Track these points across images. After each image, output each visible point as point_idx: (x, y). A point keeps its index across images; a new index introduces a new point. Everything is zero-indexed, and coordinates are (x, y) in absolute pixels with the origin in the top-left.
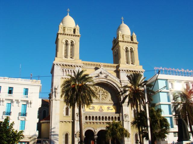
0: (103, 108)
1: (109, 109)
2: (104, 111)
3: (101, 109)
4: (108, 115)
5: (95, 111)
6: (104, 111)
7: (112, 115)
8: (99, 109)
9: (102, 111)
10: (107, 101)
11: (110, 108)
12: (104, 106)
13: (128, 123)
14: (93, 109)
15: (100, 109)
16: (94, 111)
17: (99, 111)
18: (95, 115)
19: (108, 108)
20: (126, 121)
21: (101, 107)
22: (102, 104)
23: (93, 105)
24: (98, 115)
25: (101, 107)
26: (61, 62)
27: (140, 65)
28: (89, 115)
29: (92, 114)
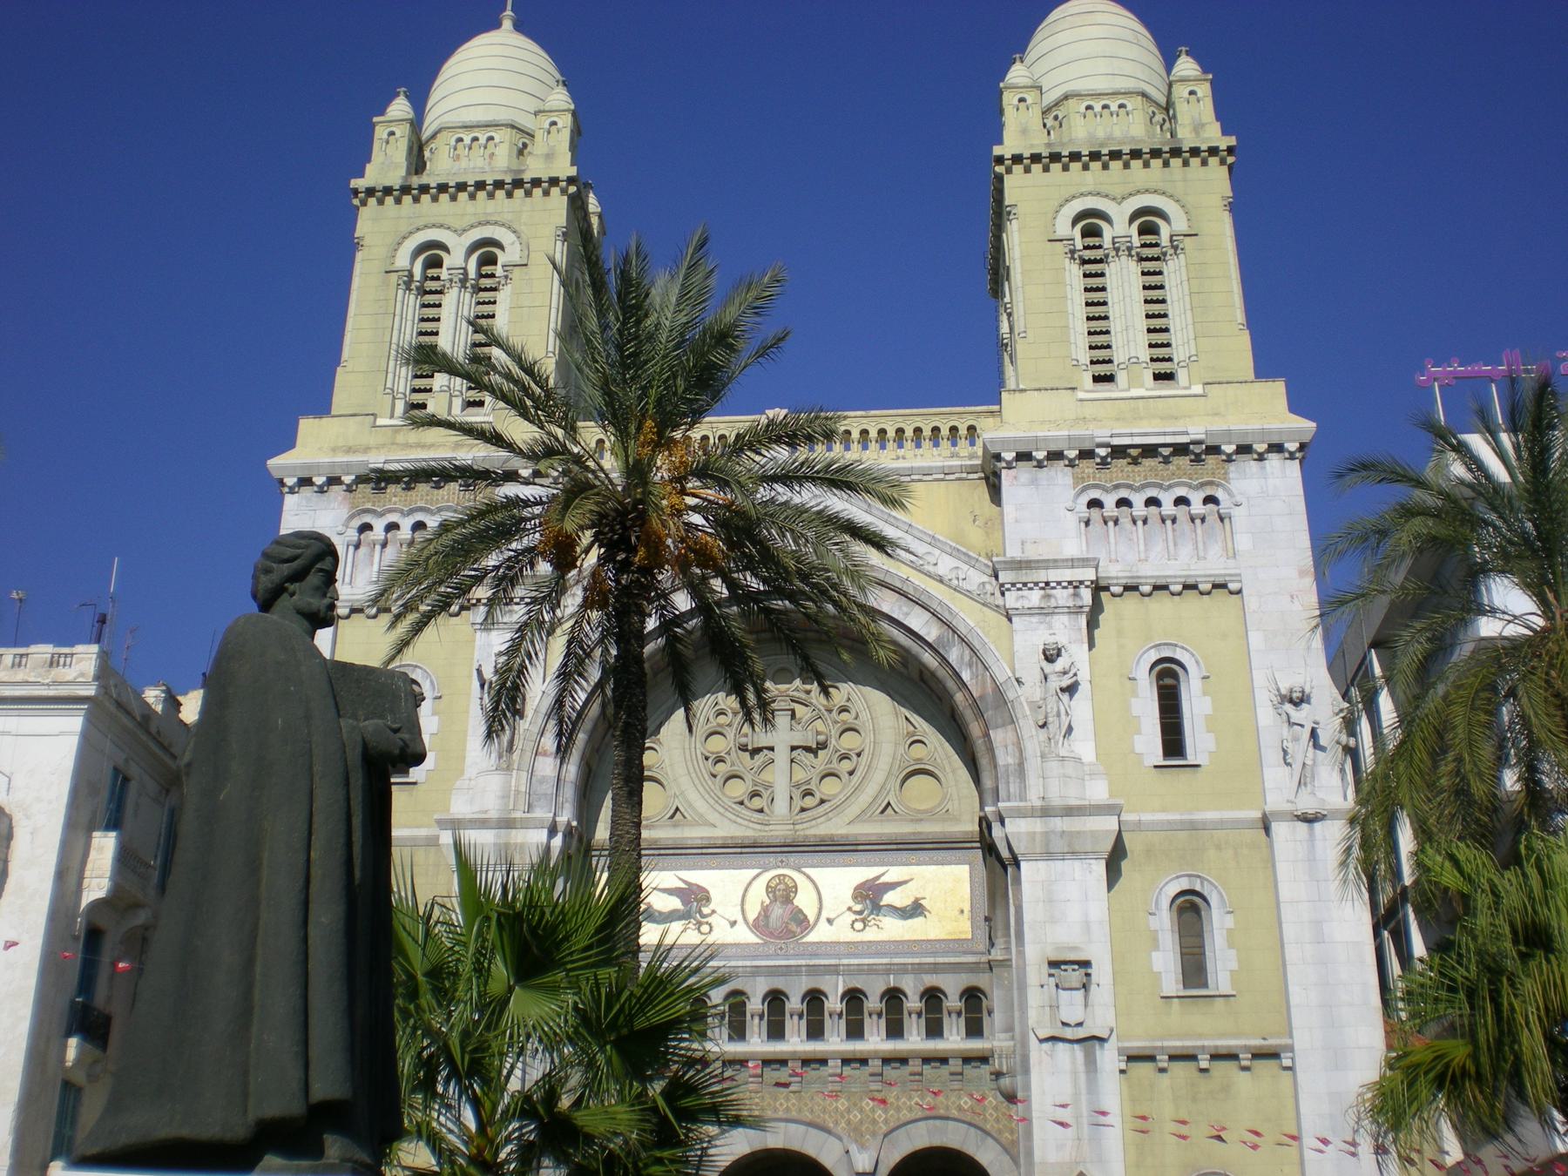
0: (805, 901)
1: (877, 908)
2: (812, 937)
3: (778, 911)
6: (812, 937)
7: (888, 970)
8: (752, 916)
10: (854, 809)
11: (889, 898)
13: (1091, 1063)
15: (765, 911)
16: (692, 937)
19: (870, 897)
20: (1053, 1039)
21: (783, 894)
22: (793, 858)
25: (783, 894)
26: (349, 450)
27: (1264, 369)
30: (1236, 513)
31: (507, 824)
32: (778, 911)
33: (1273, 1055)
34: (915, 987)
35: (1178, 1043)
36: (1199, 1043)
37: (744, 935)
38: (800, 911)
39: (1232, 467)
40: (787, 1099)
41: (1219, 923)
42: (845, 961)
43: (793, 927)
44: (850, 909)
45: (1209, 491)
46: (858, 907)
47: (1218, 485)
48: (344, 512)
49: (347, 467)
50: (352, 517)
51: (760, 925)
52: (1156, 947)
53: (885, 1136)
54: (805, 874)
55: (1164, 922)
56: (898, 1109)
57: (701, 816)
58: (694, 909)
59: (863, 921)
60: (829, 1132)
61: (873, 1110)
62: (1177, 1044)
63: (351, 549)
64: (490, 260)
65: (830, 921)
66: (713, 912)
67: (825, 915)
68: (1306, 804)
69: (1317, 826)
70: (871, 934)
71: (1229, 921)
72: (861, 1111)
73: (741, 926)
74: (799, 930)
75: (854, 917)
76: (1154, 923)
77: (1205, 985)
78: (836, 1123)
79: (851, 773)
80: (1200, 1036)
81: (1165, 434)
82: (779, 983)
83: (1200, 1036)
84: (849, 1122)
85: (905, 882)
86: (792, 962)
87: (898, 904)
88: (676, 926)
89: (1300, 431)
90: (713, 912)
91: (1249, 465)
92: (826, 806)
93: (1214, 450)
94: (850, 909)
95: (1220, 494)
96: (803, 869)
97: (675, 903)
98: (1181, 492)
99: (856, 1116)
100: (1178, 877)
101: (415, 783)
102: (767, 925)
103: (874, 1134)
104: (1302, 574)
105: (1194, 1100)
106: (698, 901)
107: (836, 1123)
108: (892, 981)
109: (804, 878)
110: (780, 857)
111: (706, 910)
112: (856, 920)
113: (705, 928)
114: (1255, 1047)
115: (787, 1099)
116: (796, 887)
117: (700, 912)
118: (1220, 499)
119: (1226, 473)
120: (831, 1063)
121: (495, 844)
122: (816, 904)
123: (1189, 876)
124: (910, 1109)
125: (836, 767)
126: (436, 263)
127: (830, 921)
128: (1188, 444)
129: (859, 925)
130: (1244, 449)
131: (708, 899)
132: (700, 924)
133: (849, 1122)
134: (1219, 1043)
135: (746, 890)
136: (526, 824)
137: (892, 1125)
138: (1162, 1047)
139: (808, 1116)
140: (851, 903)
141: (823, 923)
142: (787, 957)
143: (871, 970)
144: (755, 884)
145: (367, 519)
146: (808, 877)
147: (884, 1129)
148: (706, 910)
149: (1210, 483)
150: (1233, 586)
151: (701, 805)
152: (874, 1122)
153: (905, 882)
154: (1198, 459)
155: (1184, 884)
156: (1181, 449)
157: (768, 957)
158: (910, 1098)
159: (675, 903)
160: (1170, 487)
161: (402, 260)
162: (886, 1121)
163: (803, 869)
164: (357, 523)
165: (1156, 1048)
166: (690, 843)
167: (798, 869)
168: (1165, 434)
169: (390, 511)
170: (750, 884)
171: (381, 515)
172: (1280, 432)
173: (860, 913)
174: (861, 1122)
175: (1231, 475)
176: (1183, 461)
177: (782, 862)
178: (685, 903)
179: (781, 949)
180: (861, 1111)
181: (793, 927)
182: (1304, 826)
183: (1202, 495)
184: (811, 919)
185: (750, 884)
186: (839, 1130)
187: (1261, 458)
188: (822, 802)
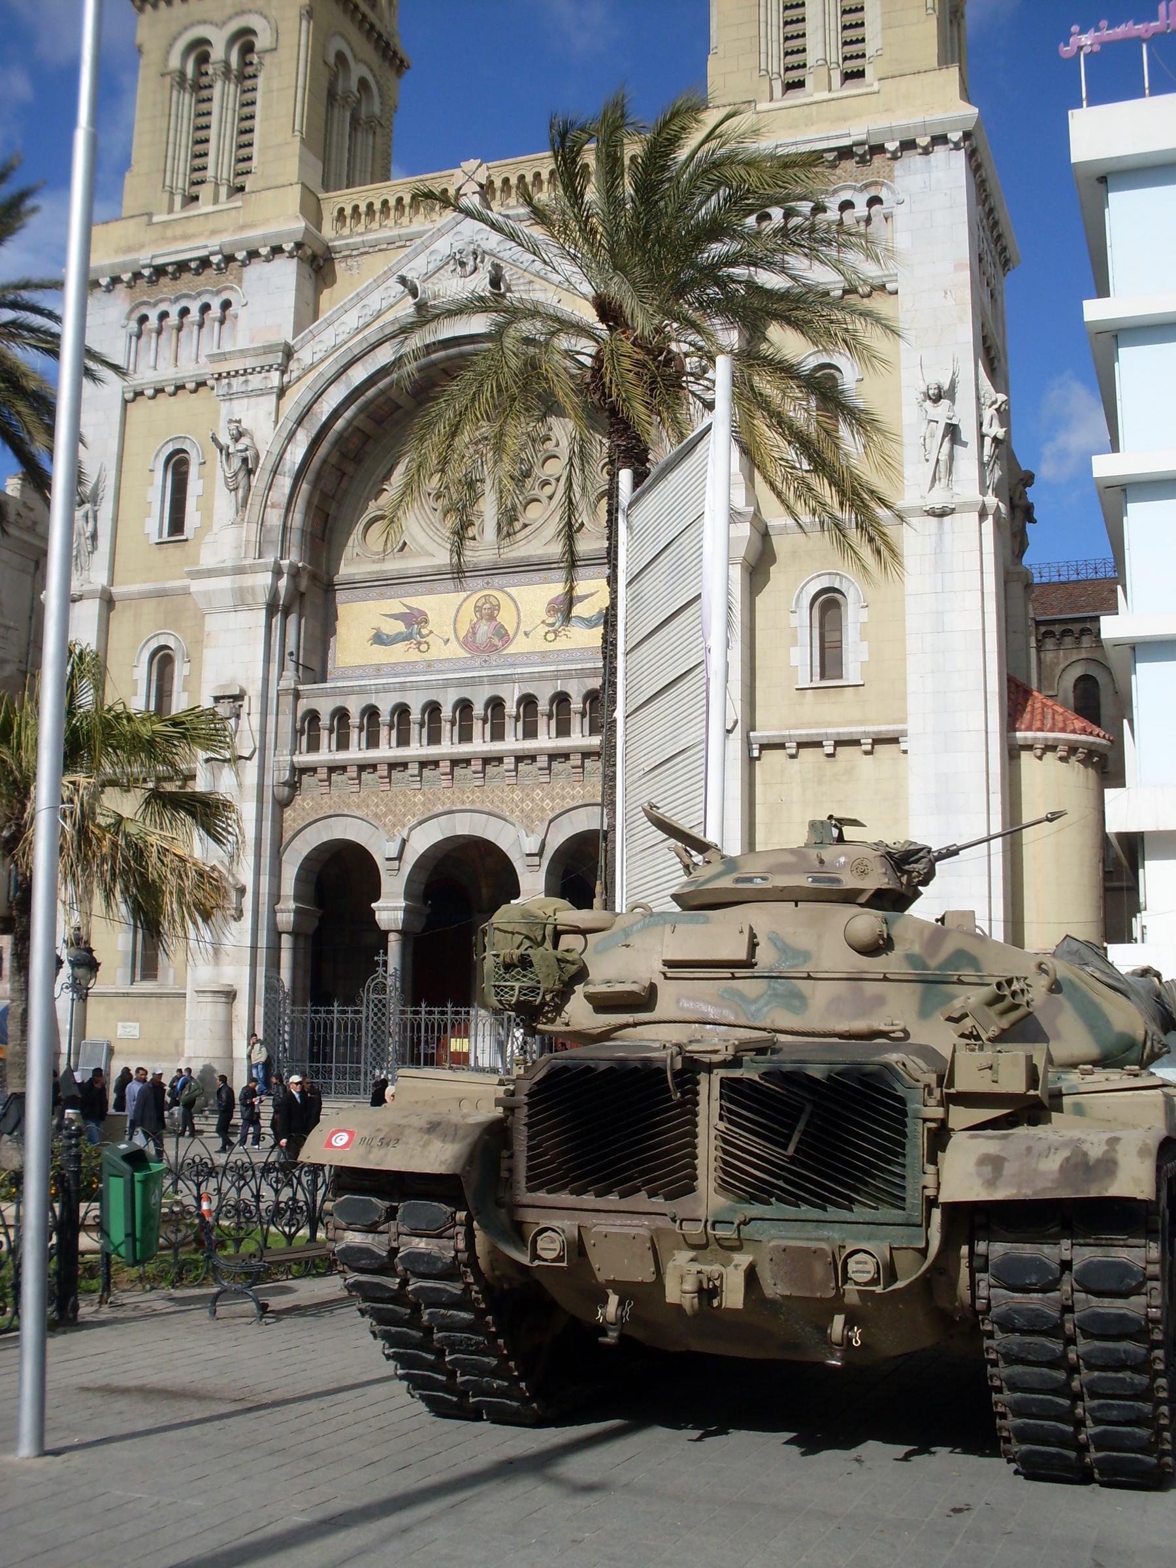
0: (506, 618)
2: (511, 649)
3: (484, 628)
4: (508, 679)
5: (432, 655)
7: (556, 676)
8: (462, 634)
9: (492, 649)
12: (512, 591)
14: (407, 638)
15: (473, 630)
16: (414, 656)
17: (462, 653)
18: (386, 689)
21: (489, 613)
22: (497, 580)
23: (407, 601)
24: (415, 687)
28: (338, 702)
29: (362, 691)
30: (898, 211)
31: (239, 570)
32: (484, 628)
33: (895, 740)
34: (579, 689)
35: (804, 732)
36: (823, 731)
37: (455, 651)
38: (503, 627)
39: (897, 165)
40: (473, 792)
41: (853, 616)
42: (519, 671)
43: (496, 641)
44: (543, 622)
45: (873, 192)
46: (551, 620)
47: (883, 184)
48: (127, 307)
49: (124, 266)
50: (132, 311)
51: (469, 642)
52: (795, 644)
53: (551, 822)
54: (506, 593)
55: (802, 620)
56: (563, 798)
57: (422, 547)
58: (415, 631)
59: (555, 632)
60: (505, 820)
61: (542, 800)
62: (804, 732)
63: (134, 339)
64: (248, 49)
65: (526, 634)
66: (431, 632)
67: (522, 628)
68: (938, 498)
69: (947, 519)
70: (561, 644)
71: (864, 615)
72: (533, 800)
73: (454, 644)
74: (500, 644)
75: (547, 629)
76: (794, 620)
77: (840, 677)
78: (512, 812)
79: (551, 498)
80: (830, 724)
81: (828, 138)
82: (466, 693)
83: (830, 724)
84: (522, 811)
85: (592, 595)
86: (476, 674)
87: (586, 615)
88: (401, 646)
89: (963, 119)
90: (431, 632)
91: (914, 159)
92: (528, 529)
93: (878, 149)
94: (543, 622)
95: (884, 194)
96: (508, 590)
97: (400, 627)
98: (846, 195)
99: (528, 805)
100: (819, 576)
101: (186, 540)
102: (474, 641)
103: (542, 820)
104: (958, 267)
105: (820, 782)
106: (418, 624)
107: (512, 812)
108: (559, 686)
109: (506, 597)
110: (487, 579)
111: (424, 631)
112: (548, 632)
113: (424, 647)
114: (874, 733)
115: (473, 792)
116: (499, 605)
117: (419, 633)
118: (884, 198)
119: (892, 171)
120: (506, 760)
121: (232, 589)
122: (515, 620)
123: (830, 574)
124: (573, 798)
125: (536, 492)
126: (204, 59)
127: (526, 634)
128: (851, 147)
129: (551, 636)
130: (908, 145)
131: (426, 622)
132: (419, 643)
133: (522, 811)
134: (841, 730)
135: (458, 611)
136: (253, 569)
137: (558, 812)
138: (790, 736)
139: (488, 807)
140: (545, 617)
141: (521, 633)
142: (490, 668)
143: (541, 677)
144: (465, 604)
145: (144, 310)
146: (509, 596)
147: (551, 815)
148: (424, 631)
149: (875, 183)
150: (889, 287)
151: (422, 538)
152: (543, 810)
153: (592, 595)
154: (863, 161)
155: (824, 583)
156: (845, 153)
157: (473, 669)
158: (573, 788)
159: (400, 627)
160: (835, 192)
161: (175, 62)
162: (553, 809)
163: (508, 590)
164: (136, 315)
165: (784, 736)
166: (410, 573)
167: (501, 589)
168: (828, 138)
169: (162, 301)
170: (461, 605)
171: (155, 305)
172: (942, 123)
173: (553, 625)
174: (532, 810)
175: (896, 173)
176: (849, 165)
177: (488, 583)
178: (409, 625)
179: (485, 661)
180: (533, 800)
181: (496, 641)
182: (934, 520)
183: (866, 196)
184: (511, 633)
185: (461, 605)
186: (513, 818)
187: (926, 151)
188: (525, 526)
